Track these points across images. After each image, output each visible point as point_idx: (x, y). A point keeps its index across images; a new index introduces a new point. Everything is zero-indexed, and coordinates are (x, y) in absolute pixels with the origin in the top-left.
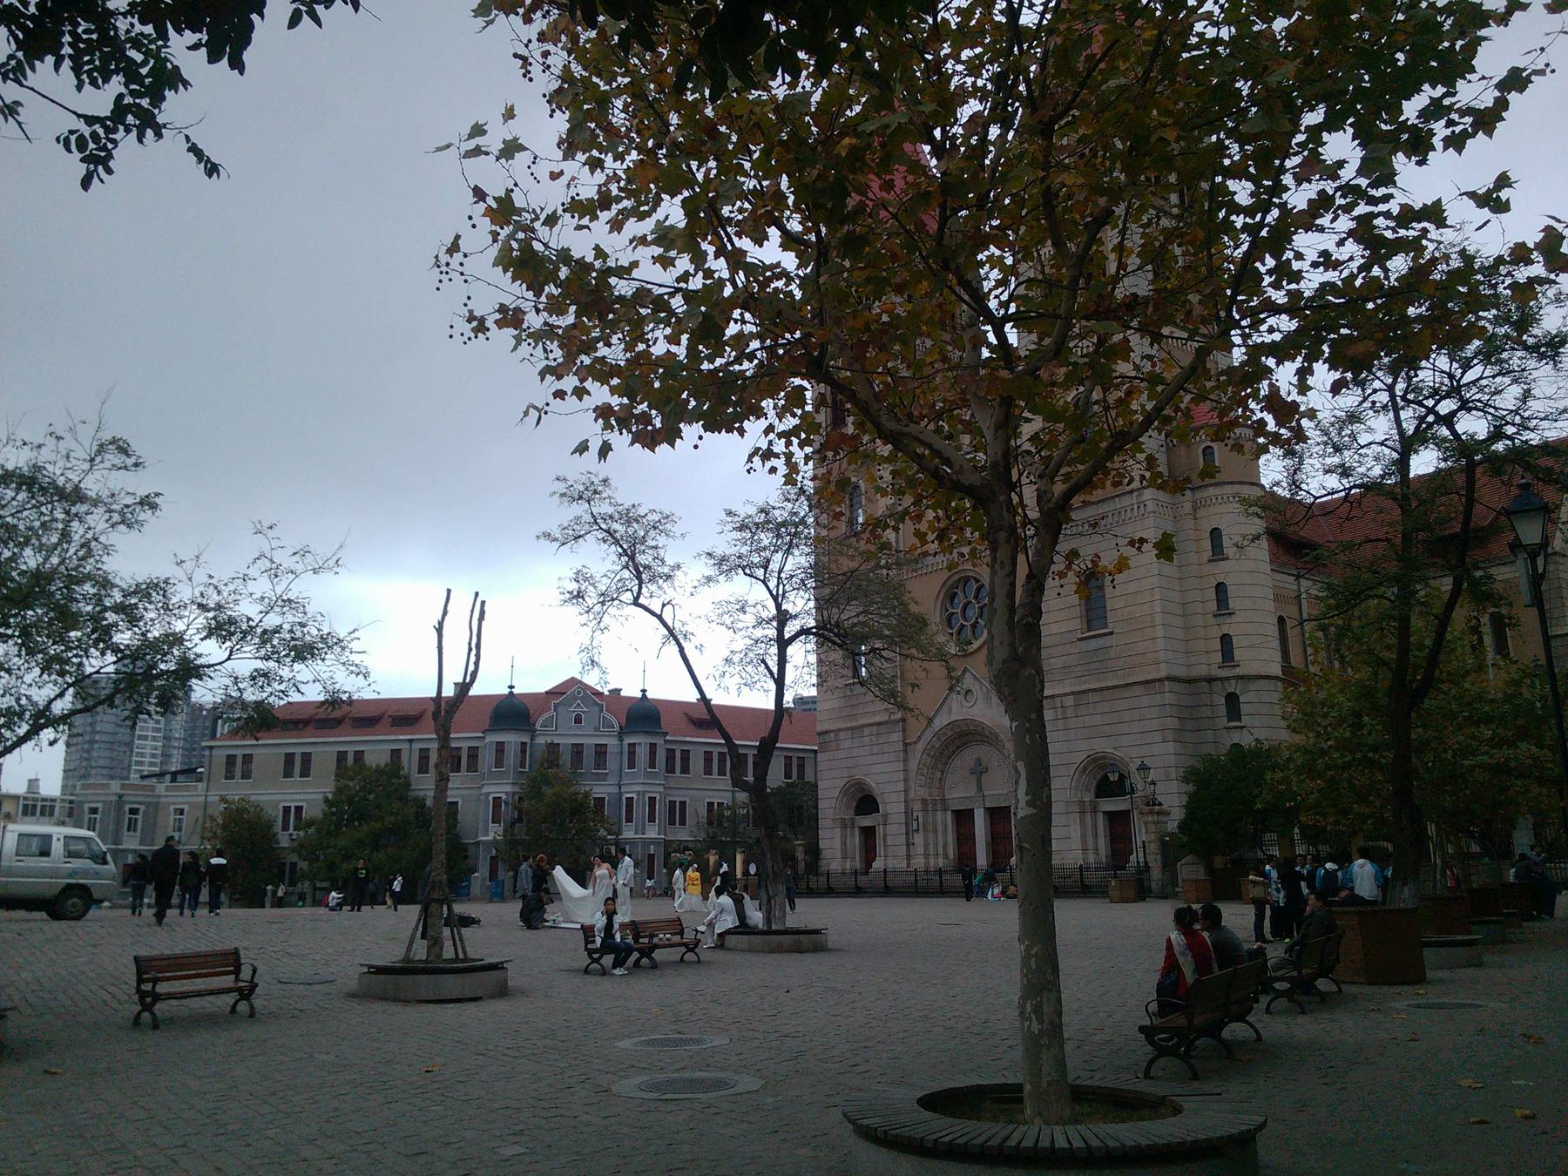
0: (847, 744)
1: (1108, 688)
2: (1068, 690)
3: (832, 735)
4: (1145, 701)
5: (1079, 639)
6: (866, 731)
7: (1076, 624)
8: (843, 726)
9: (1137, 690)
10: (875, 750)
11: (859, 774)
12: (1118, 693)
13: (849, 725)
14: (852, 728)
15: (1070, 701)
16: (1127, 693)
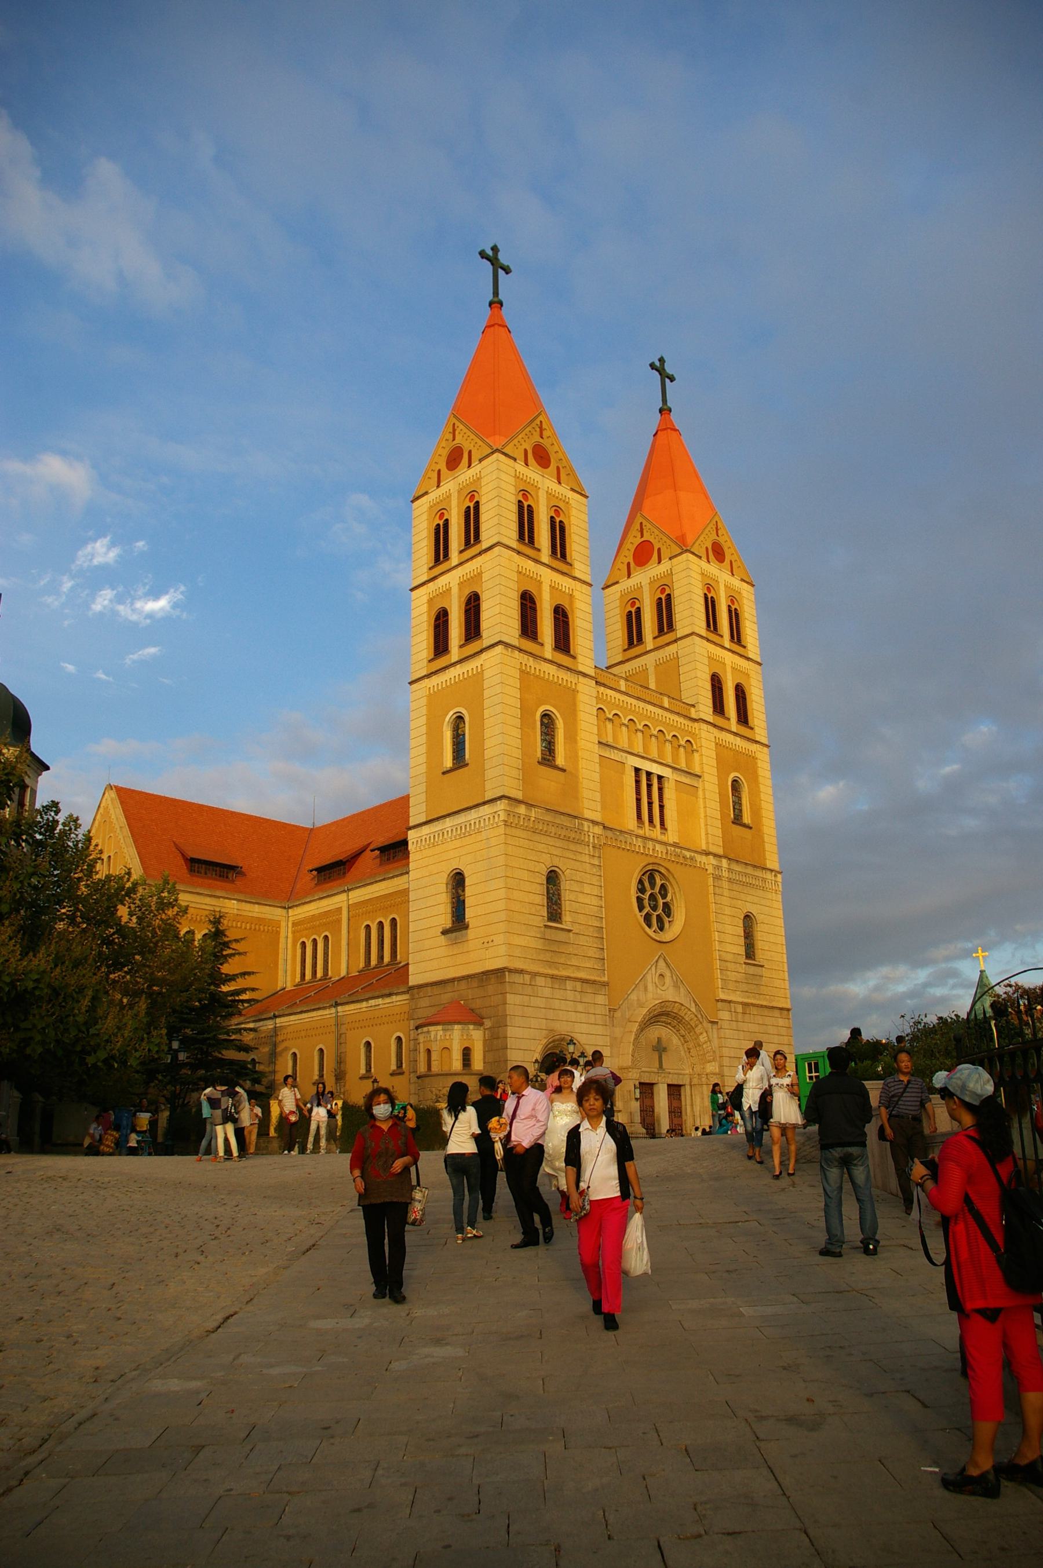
0: (547, 992)
1: (762, 1006)
2: (740, 1000)
3: (527, 977)
4: (781, 1022)
5: (745, 963)
6: (569, 985)
7: (742, 950)
8: (542, 970)
9: (777, 1013)
10: (580, 1007)
11: (563, 1028)
12: (766, 1012)
13: (550, 972)
14: (553, 977)
15: (740, 1009)
16: (770, 1013)
